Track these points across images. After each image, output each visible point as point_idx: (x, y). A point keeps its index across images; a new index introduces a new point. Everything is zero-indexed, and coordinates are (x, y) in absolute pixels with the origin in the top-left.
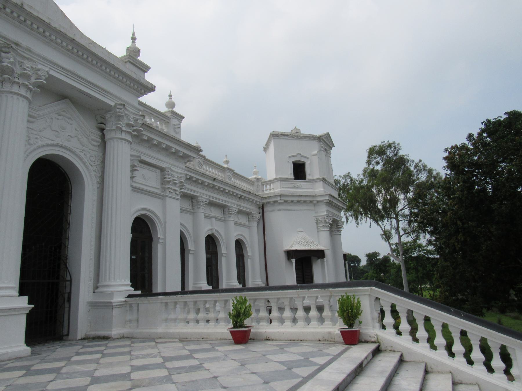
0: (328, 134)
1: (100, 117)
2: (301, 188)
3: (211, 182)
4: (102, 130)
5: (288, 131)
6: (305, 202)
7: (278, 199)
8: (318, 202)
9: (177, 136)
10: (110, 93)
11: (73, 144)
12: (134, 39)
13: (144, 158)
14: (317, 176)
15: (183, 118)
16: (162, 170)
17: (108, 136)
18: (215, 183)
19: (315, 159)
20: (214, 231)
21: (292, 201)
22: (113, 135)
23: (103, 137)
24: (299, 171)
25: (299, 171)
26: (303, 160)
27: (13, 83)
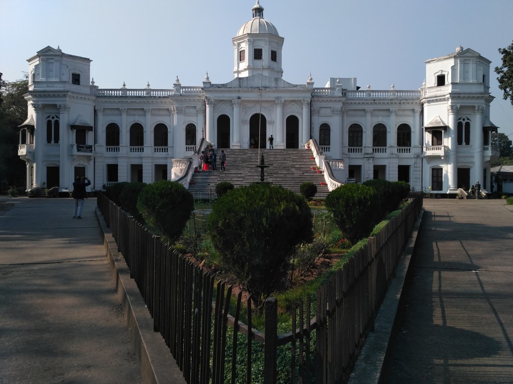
3: (373, 102)
8: (448, 98)
18: (375, 102)
20: (380, 122)
24: (441, 80)
26: (443, 73)
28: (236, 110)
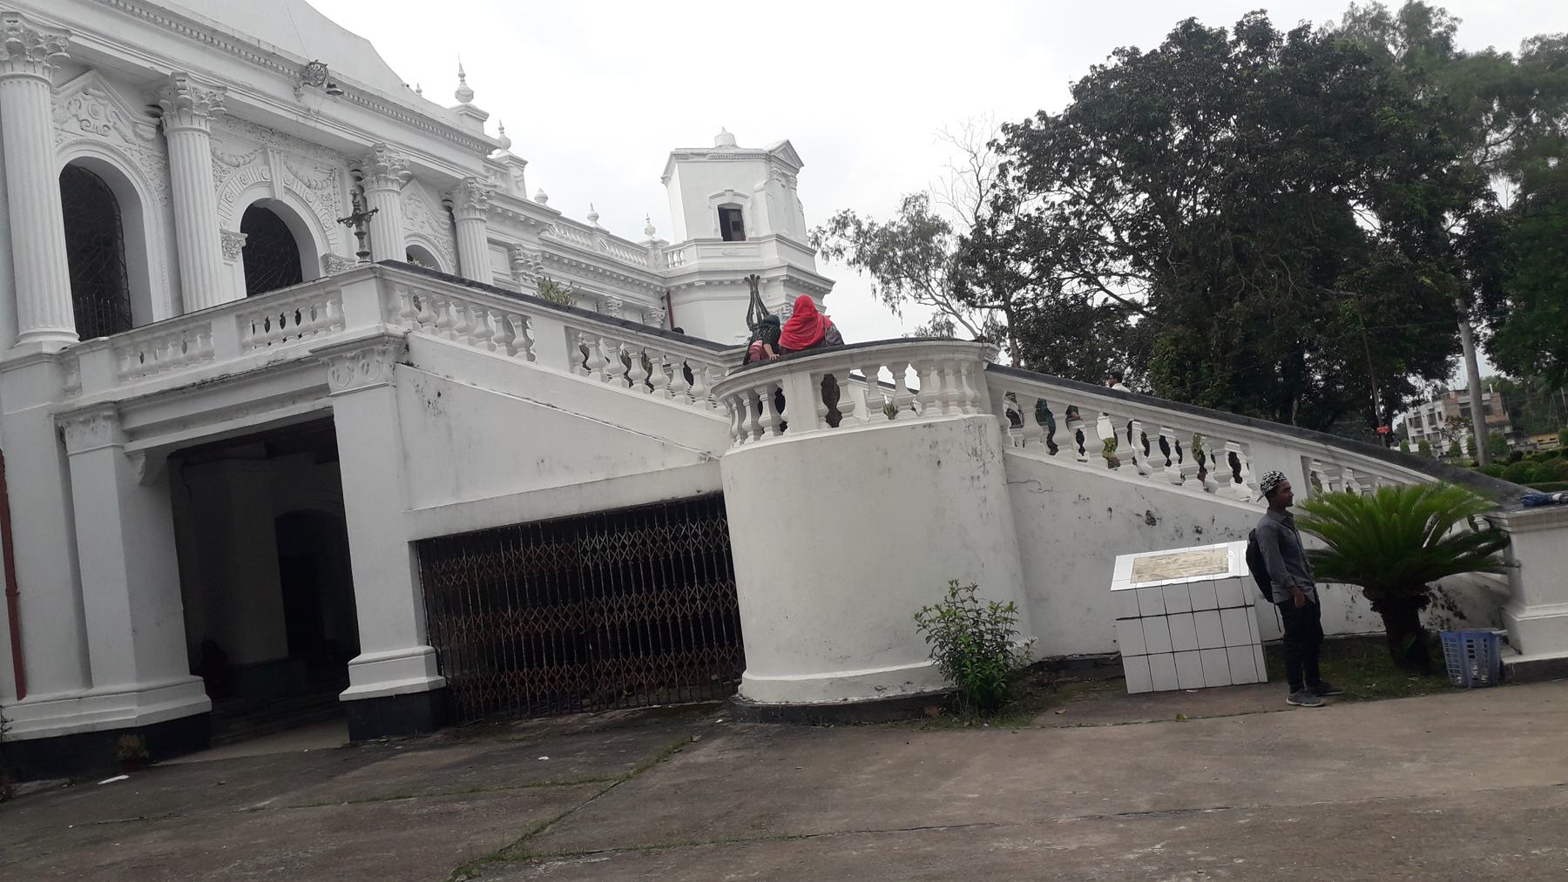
1: (450, 199)
2: (737, 257)
5: (707, 143)
7: (697, 278)
9: (516, 194)
11: (427, 231)
12: (462, 76)
14: (765, 230)
16: (510, 248)
19: (761, 198)
21: (721, 283)
22: (465, 215)
23: (452, 217)
24: (731, 224)
25: (731, 224)
26: (738, 201)
27: (387, 180)
28: (197, 148)
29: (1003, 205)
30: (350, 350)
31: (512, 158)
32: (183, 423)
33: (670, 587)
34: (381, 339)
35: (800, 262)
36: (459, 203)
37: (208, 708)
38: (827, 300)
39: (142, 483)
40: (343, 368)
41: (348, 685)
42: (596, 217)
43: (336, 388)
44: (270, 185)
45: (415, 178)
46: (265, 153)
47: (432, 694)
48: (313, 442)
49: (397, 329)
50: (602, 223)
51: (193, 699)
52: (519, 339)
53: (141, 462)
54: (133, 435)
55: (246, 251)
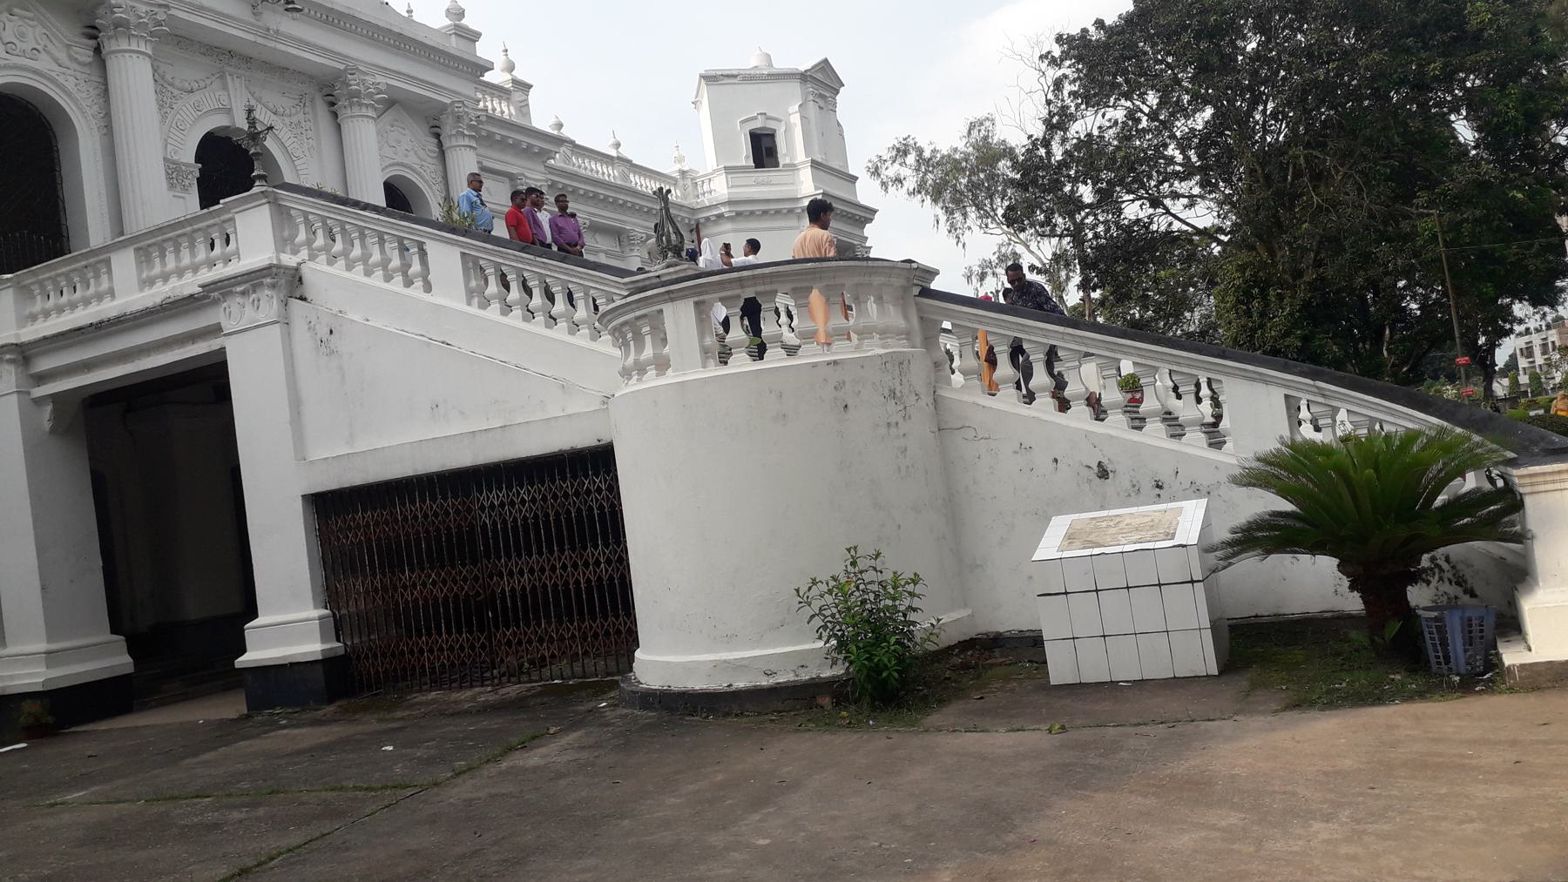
0: (826, 61)
1: (435, 122)
4: (438, 136)
6: (778, 212)
10: (444, 86)
11: (412, 160)
13: (487, 164)
15: (530, 86)
17: (446, 144)
19: (796, 119)
21: (752, 213)
23: (440, 145)
24: (764, 149)
25: (764, 149)
26: (771, 125)
27: (360, 105)
28: (133, 72)
29: (1057, 122)
30: (239, 284)
31: (515, 82)
32: (87, 366)
33: (573, 549)
34: (267, 271)
35: (837, 189)
36: (448, 129)
37: (131, 670)
38: (868, 230)
39: (53, 431)
40: (234, 304)
41: (243, 651)
42: (618, 145)
43: (228, 326)
44: (229, 111)
45: (392, 103)
46: (222, 77)
47: (327, 663)
48: (207, 384)
49: (289, 260)
50: (625, 152)
51: (118, 661)
52: (416, 267)
53: (49, 408)
54: (41, 378)
55: (201, 182)
